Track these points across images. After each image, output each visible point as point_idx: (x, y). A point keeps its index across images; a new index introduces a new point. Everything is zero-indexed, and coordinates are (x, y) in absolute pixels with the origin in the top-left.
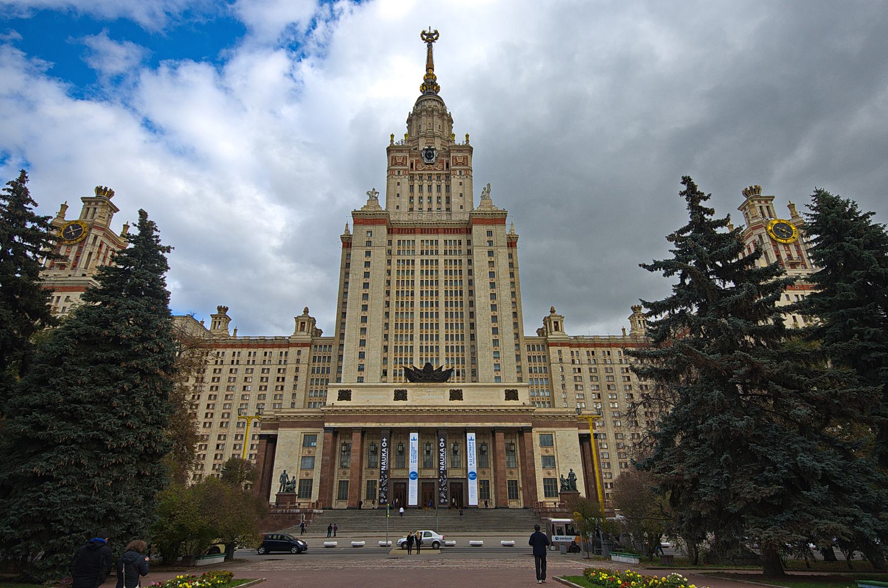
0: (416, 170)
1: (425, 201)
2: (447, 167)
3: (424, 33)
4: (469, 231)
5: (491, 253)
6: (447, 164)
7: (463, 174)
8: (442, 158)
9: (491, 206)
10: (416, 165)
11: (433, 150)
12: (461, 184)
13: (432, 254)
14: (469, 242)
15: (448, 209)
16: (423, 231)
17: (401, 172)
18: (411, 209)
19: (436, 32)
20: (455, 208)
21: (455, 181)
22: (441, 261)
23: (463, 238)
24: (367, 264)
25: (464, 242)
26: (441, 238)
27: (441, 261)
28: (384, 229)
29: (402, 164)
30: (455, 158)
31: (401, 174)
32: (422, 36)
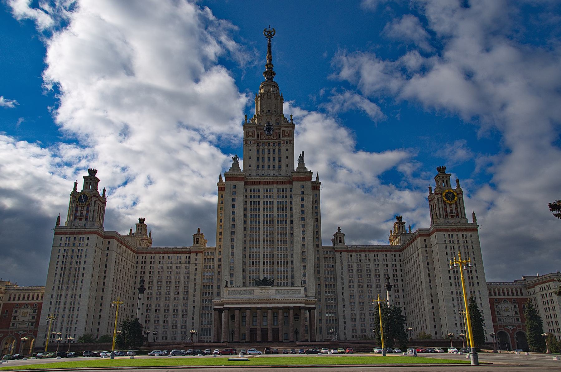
0: (261, 139)
1: (266, 160)
2: (279, 137)
3: (265, 30)
4: (291, 183)
5: (303, 199)
6: (279, 135)
7: (288, 143)
11: (271, 126)
12: (287, 150)
13: (270, 197)
14: (291, 190)
15: (280, 166)
16: (264, 183)
18: (258, 167)
19: (274, 30)
20: (283, 166)
21: (283, 148)
23: (287, 187)
24: (234, 206)
25: (288, 190)
26: (275, 187)
28: (243, 183)
29: (252, 137)
31: (252, 143)
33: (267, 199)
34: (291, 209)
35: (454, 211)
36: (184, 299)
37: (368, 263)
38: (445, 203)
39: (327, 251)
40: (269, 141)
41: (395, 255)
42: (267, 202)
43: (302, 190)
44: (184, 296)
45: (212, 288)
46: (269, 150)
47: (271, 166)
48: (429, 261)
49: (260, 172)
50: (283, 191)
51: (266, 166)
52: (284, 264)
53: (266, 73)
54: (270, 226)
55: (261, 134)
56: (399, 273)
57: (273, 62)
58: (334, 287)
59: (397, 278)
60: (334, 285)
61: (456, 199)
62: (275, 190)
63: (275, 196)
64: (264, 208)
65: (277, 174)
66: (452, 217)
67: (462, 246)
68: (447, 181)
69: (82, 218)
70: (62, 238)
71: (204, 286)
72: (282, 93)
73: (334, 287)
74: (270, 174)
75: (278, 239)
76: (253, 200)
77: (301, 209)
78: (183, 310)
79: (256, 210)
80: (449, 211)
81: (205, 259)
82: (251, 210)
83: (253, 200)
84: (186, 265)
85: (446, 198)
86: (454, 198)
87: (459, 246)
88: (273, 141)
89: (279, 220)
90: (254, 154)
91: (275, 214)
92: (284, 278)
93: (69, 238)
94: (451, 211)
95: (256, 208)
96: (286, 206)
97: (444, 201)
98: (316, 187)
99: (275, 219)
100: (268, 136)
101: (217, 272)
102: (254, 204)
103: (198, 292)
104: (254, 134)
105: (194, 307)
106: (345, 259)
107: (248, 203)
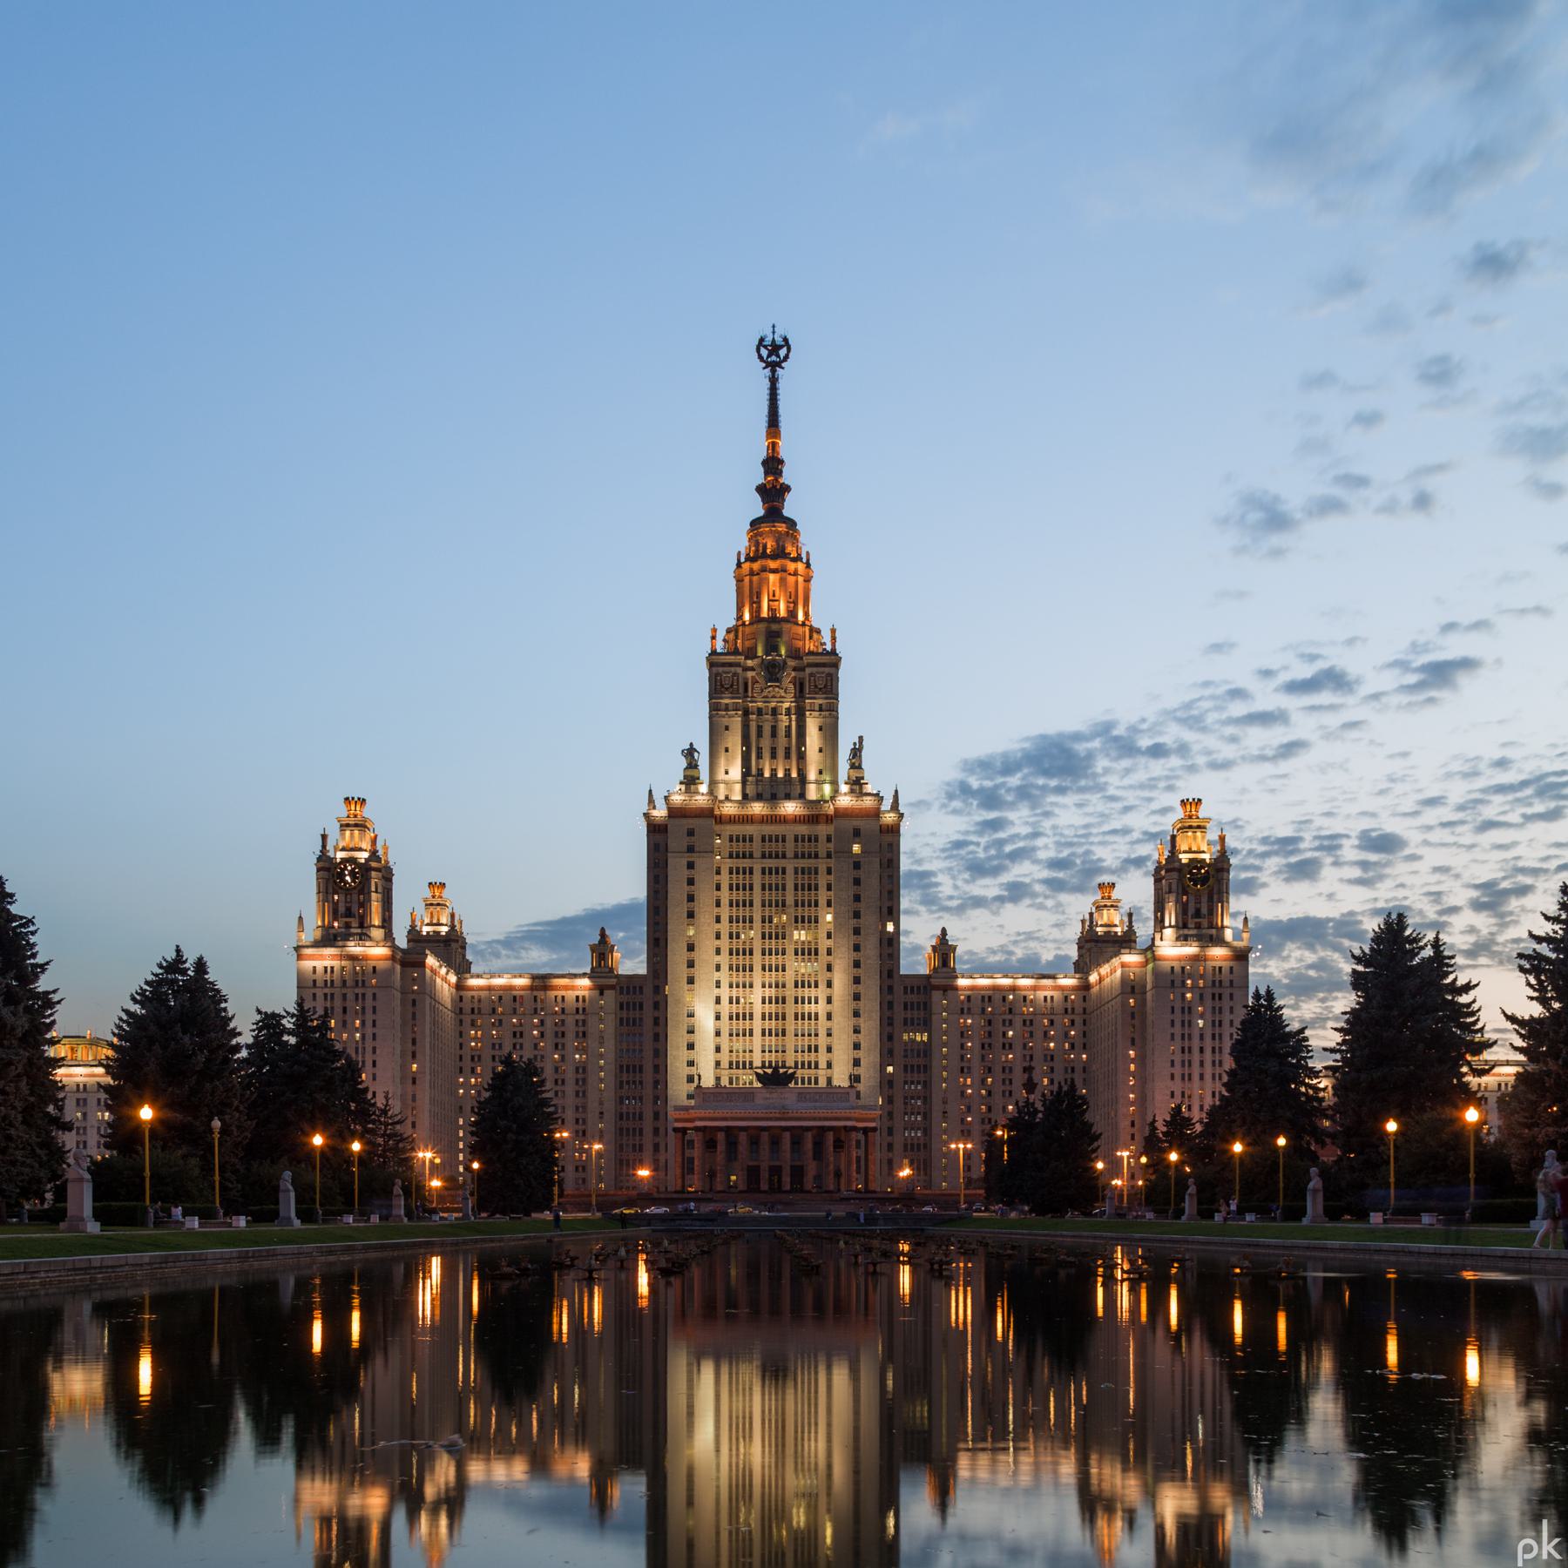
6: (802, 685)
10: (753, 689)
22: (790, 871)
27: (790, 871)
33: (770, 860)
39: (912, 988)
42: (770, 869)
44: (577, 1088)
45: (641, 1071)
53: (761, 489)
57: (783, 453)
58: (925, 1072)
60: (925, 1066)
62: (789, 839)
71: (621, 1067)
72: (808, 553)
73: (925, 1072)
77: (852, 890)
84: (577, 1017)
91: (790, 900)
101: (651, 1034)
105: (601, 1113)
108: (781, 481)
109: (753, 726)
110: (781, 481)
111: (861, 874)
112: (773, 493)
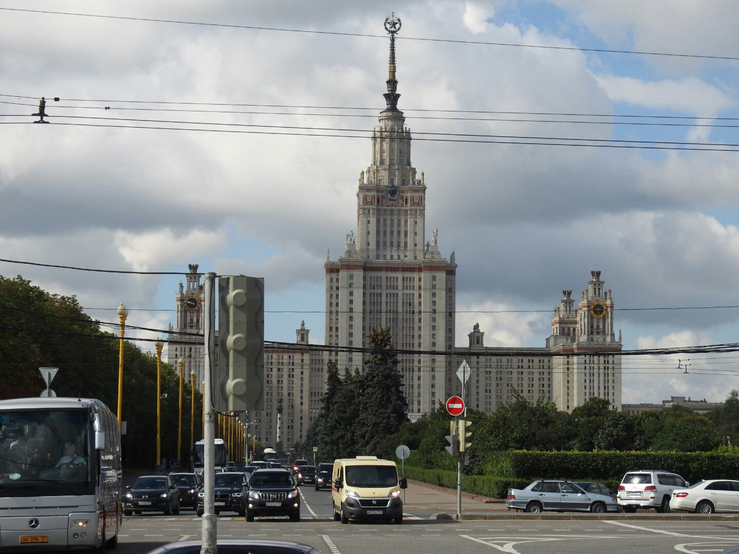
0: (382, 206)
4: (420, 270)
6: (406, 200)
8: (402, 194)
9: (439, 253)
11: (396, 187)
13: (394, 289)
14: (420, 280)
17: (371, 210)
19: (399, 20)
23: (416, 275)
25: (417, 279)
26: (399, 275)
30: (412, 198)
31: (371, 213)
32: (385, 25)
34: (420, 303)
35: (601, 326)
36: (289, 408)
37: (510, 370)
38: (592, 317)
40: (393, 208)
41: (543, 360)
43: (434, 283)
44: (289, 404)
46: (392, 220)
47: (395, 244)
48: (569, 379)
49: (381, 253)
50: (410, 281)
51: (388, 244)
52: (409, 371)
54: (393, 324)
55: (383, 197)
56: (546, 383)
57: (396, 78)
59: (543, 389)
61: (604, 313)
63: (400, 287)
64: (387, 302)
65: (402, 257)
66: (598, 333)
67: (602, 366)
68: (599, 289)
69: (193, 326)
70: (176, 348)
71: (312, 393)
72: (409, 129)
74: (393, 256)
75: (403, 341)
76: (373, 291)
78: (289, 420)
79: (377, 305)
80: (595, 326)
81: (312, 360)
82: (370, 305)
83: (373, 291)
85: (594, 311)
86: (602, 311)
87: (599, 368)
88: (398, 208)
89: (405, 317)
90: (373, 228)
91: (400, 310)
92: (409, 388)
93: (185, 348)
94: (598, 326)
95: (377, 302)
96: (413, 300)
97: (591, 315)
98: (450, 271)
99: (400, 316)
100: (391, 202)
102: (374, 296)
103: (306, 400)
104: (373, 199)
106: (481, 364)
107: (368, 295)
108: (396, 93)
109: (382, 220)
110: (396, 93)
111: (436, 299)
112: (392, 98)
